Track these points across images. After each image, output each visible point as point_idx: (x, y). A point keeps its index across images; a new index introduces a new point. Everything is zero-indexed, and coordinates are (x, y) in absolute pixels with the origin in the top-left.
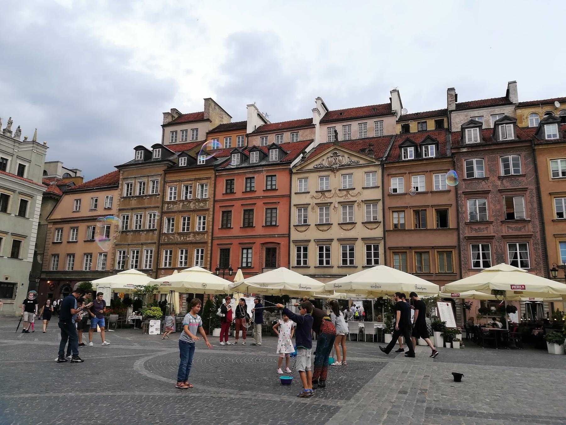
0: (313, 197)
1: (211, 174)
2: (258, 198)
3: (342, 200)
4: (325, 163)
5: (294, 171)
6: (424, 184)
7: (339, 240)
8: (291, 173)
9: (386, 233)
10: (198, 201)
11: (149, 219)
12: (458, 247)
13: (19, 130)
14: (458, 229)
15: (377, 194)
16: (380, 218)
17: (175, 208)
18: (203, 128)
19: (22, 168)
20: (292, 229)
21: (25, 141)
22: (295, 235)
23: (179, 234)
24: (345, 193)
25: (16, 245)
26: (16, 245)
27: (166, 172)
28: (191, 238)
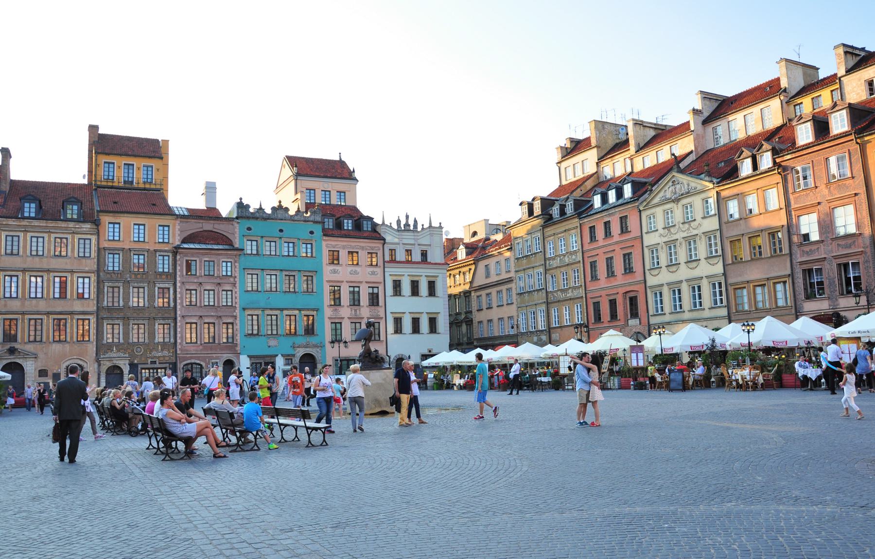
0: (661, 235)
1: (576, 222)
2: (617, 243)
3: (685, 235)
4: (668, 196)
5: (641, 209)
6: (737, 209)
7: (687, 280)
8: (640, 211)
9: (727, 268)
10: (571, 253)
11: (533, 279)
12: (792, 275)
13: (415, 221)
14: (791, 254)
15: (712, 224)
16: (720, 252)
17: (555, 263)
18: (591, 156)
19: (424, 254)
20: (647, 272)
21: (423, 229)
22: (651, 281)
23: (562, 290)
24: (687, 226)
25: (433, 322)
26: (433, 322)
27: (544, 227)
28: (570, 294)
